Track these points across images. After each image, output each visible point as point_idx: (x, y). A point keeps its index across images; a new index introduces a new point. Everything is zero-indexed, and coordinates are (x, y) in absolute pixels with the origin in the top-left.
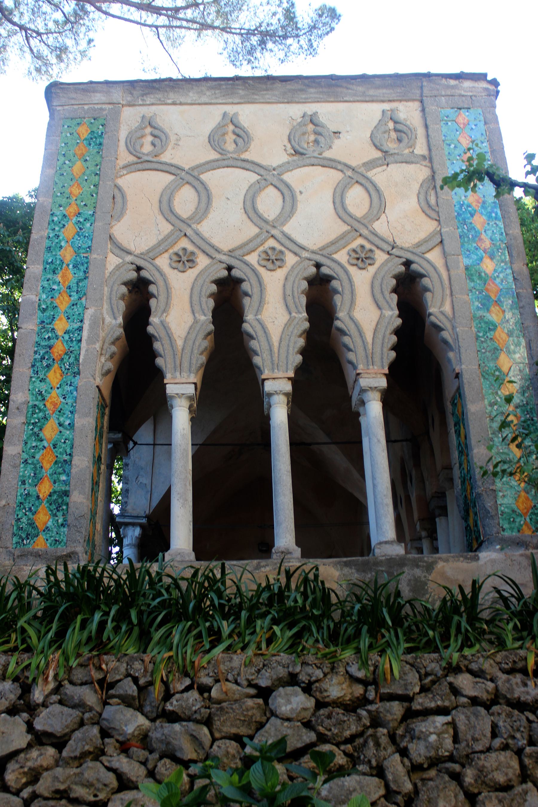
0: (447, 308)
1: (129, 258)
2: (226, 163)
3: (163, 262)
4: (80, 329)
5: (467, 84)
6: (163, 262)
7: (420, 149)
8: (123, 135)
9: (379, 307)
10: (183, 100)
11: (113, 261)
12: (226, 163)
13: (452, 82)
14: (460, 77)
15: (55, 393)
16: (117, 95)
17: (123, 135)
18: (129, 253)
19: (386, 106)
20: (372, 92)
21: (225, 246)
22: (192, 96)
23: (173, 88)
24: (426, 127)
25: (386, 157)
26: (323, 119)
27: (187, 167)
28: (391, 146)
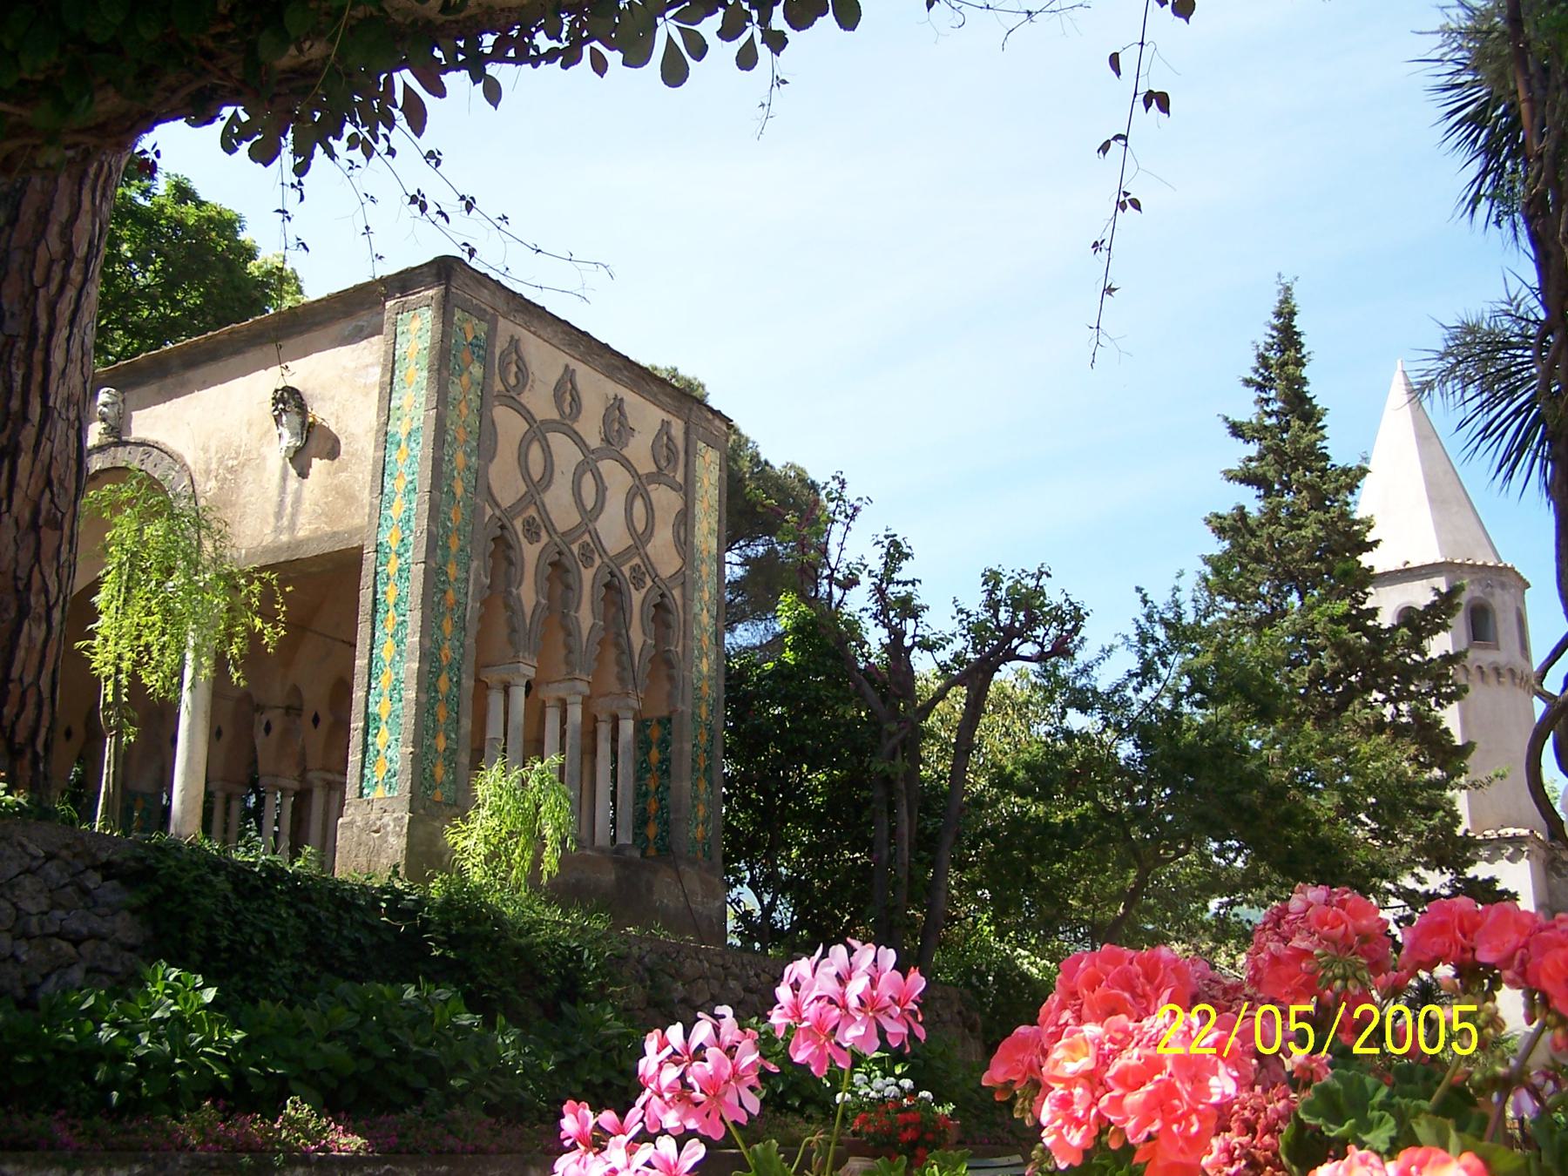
0: (679, 649)
1: (498, 513)
2: (564, 428)
3: (518, 524)
4: (467, 580)
5: (717, 422)
6: (518, 524)
7: (679, 478)
8: (497, 352)
9: (644, 633)
10: (541, 332)
11: (489, 511)
12: (564, 428)
13: (710, 416)
14: (717, 414)
15: (448, 644)
16: (501, 304)
17: (497, 352)
18: (498, 505)
19: (666, 416)
20: (661, 397)
21: (561, 528)
22: (548, 332)
23: (539, 316)
24: (686, 452)
25: (658, 477)
26: (627, 409)
27: (538, 418)
28: (663, 463)
